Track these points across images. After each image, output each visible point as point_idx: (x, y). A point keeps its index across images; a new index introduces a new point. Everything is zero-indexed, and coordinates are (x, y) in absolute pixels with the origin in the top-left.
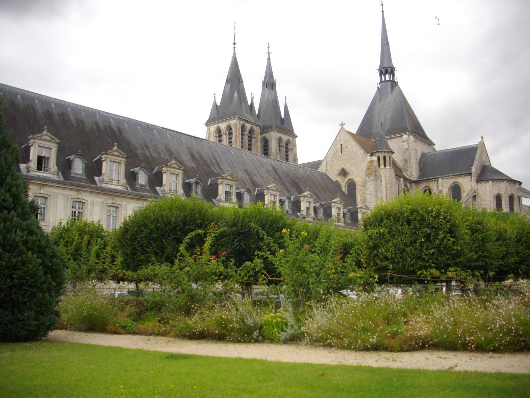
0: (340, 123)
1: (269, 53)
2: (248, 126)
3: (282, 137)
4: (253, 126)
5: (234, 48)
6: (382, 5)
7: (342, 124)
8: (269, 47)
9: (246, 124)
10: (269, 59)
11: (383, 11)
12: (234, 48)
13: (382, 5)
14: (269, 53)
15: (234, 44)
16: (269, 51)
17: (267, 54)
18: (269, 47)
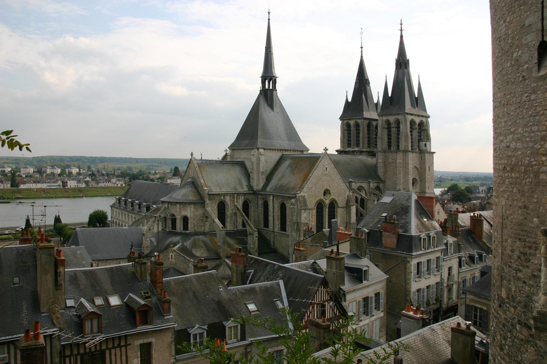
3: (389, 118)
15: (362, 48)
17: (400, 32)
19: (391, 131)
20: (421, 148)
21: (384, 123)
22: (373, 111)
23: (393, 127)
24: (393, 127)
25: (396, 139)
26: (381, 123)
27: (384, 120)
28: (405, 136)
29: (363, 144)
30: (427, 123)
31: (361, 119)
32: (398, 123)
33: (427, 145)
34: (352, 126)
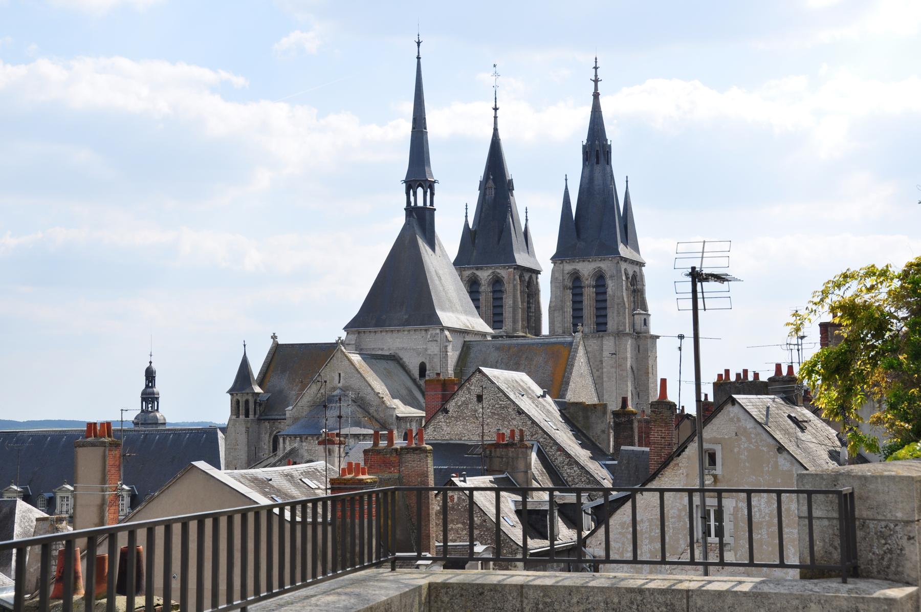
0: (276, 335)
1: (596, 81)
2: (484, 275)
3: (578, 268)
4: (498, 271)
5: (496, 117)
6: (419, 43)
7: (274, 337)
8: (596, 68)
9: (479, 273)
10: (596, 96)
11: (419, 58)
12: (496, 117)
13: (419, 43)
14: (596, 81)
16: (596, 76)
18: (596, 68)
19: (581, 294)
20: (638, 328)
21: (567, 276)
22: (523, 251)
23: (589, 286)
24: (589, 286)
25: (593, 311)
26: (561, 278)
27: (567, 272)
28: (618, 304)
29: (515, 322)
30: (642, 276)
31: (510, 267)
32: (600, 279)
33: (647, 322)
34: (483, 282)
